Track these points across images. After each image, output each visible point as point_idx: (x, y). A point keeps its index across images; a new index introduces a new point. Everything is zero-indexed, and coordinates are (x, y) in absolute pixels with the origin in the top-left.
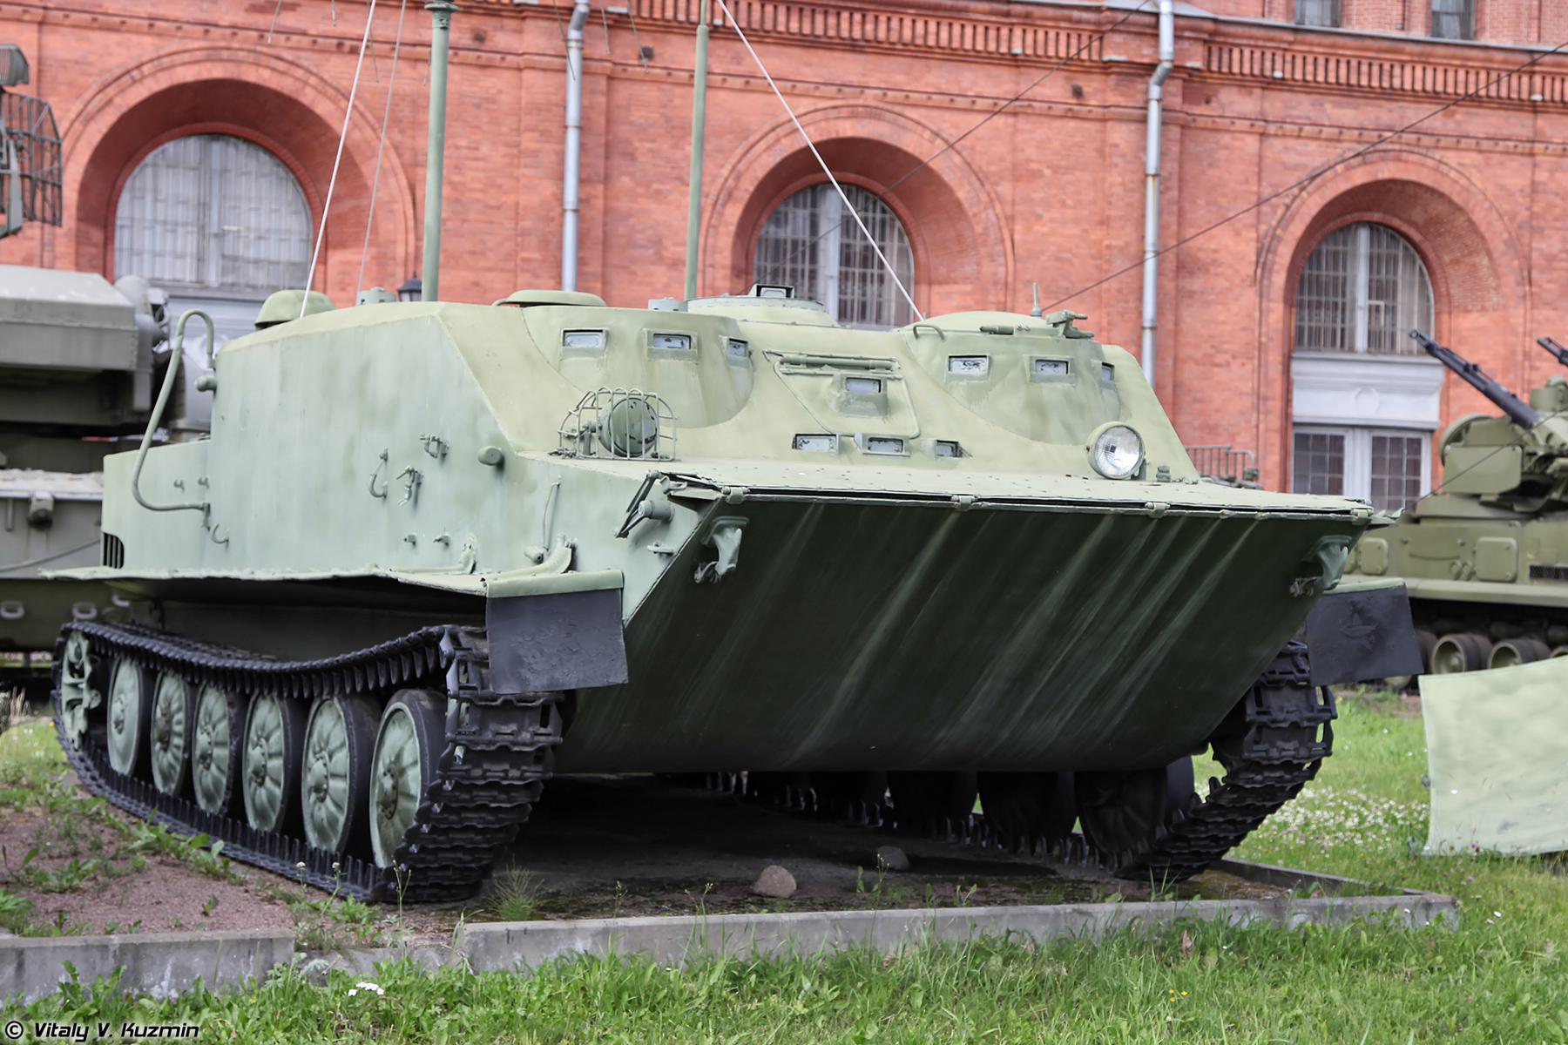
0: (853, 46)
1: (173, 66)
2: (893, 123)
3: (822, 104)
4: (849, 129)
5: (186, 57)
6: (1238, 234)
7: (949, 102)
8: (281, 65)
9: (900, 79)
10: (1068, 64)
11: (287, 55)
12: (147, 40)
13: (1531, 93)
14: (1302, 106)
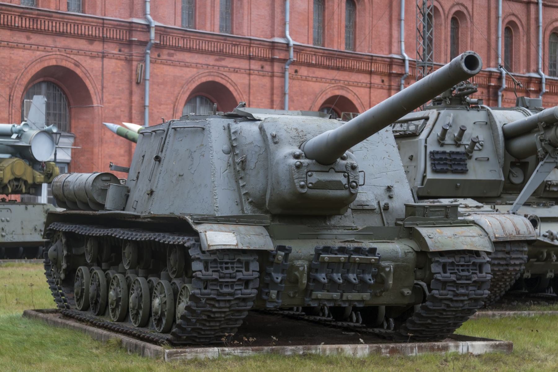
0: (338, 69)
1: (201, 77)
2: (346, 91)
3: (332, 85)
5: (204, 75)
7: (357, 85)
8: (223, 77)
9: (347, 78)
10: (381, 74)
11: (224, 73)
12: (195, 70)
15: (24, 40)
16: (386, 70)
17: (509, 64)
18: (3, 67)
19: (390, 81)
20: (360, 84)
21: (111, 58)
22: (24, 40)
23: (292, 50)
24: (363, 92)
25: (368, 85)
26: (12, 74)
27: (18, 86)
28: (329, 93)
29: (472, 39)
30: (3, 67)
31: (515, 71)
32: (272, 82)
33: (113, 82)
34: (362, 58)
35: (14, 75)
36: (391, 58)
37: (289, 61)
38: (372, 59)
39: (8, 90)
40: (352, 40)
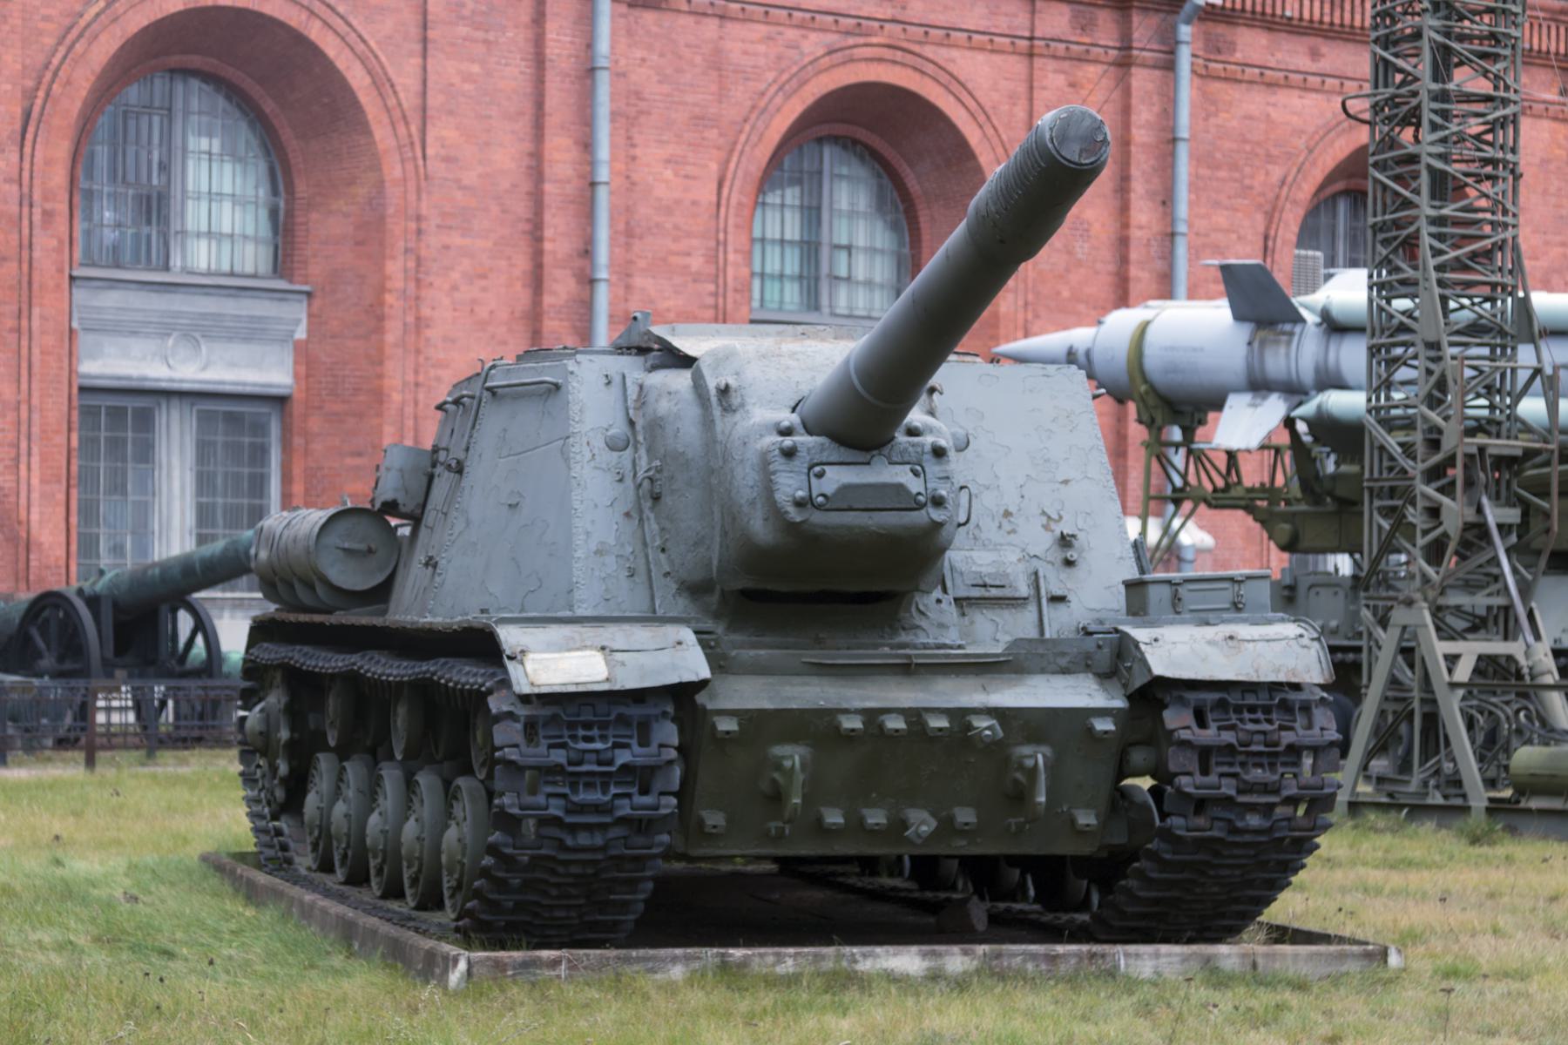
15: (1303, 62)
18: (1248, 148)
21: (1540, 117)
22: (1304, 62)
26: (1270, 167)
27: (1288, 206)
30: (1248, 148)
33: (1545, 192)
35: (1277, 172)
39: (1260, 219)
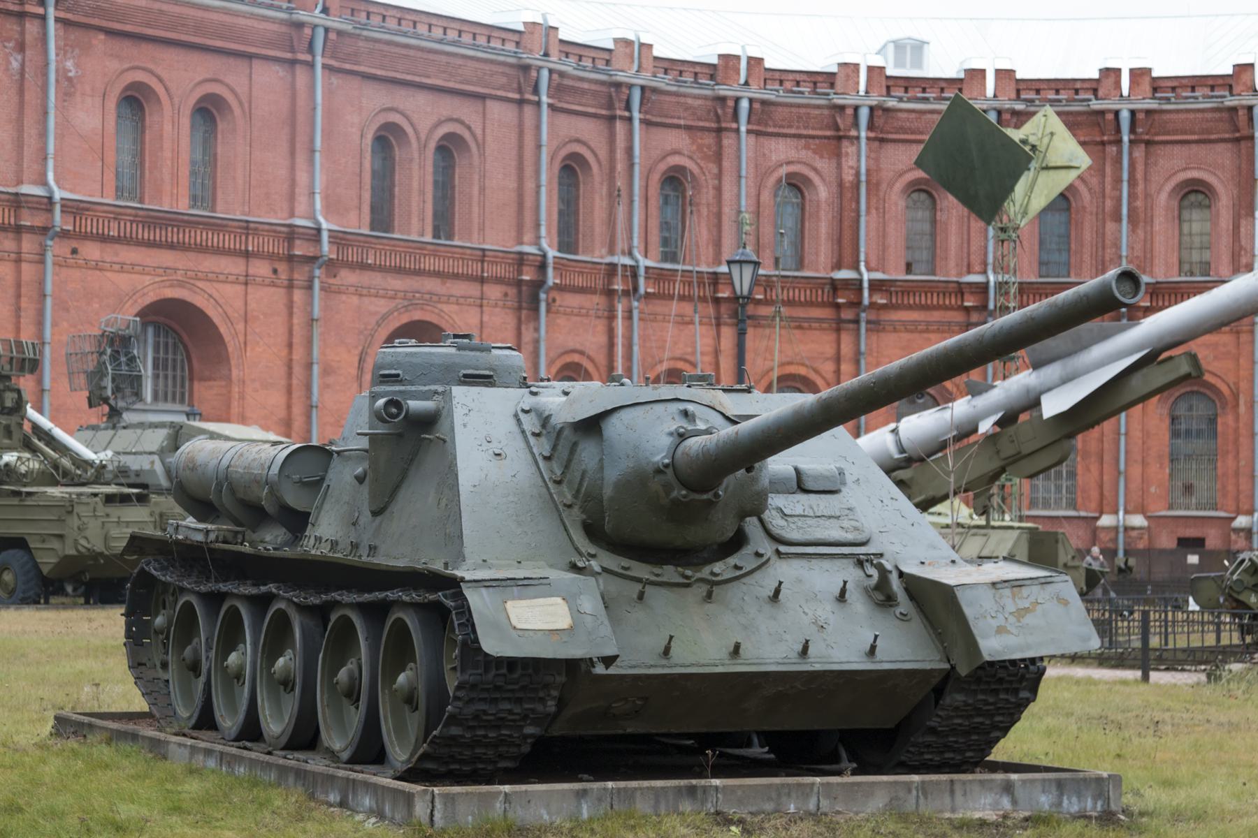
0: (171, 246)
2: (190, 289)
3: (158, 279)
4: (170, 293)
6: (349, 351)
7: (216, 278)
10: (271, 257)
13: (483, 271)
14: (376, 279)
16: (282, 249)
17: (568, 242)
19: (292, 270)
20: (222, 277)
23: (58, 208)
24: (232, 292)
25: (242, 279)
28: (151, 294)
29: (482, 189)
31: (584, 253)
32: (19, 272)
34: (226, 226)
36: (290, 226)
37: (51, 232)
38: (247, 228)
40: (205, 191)
